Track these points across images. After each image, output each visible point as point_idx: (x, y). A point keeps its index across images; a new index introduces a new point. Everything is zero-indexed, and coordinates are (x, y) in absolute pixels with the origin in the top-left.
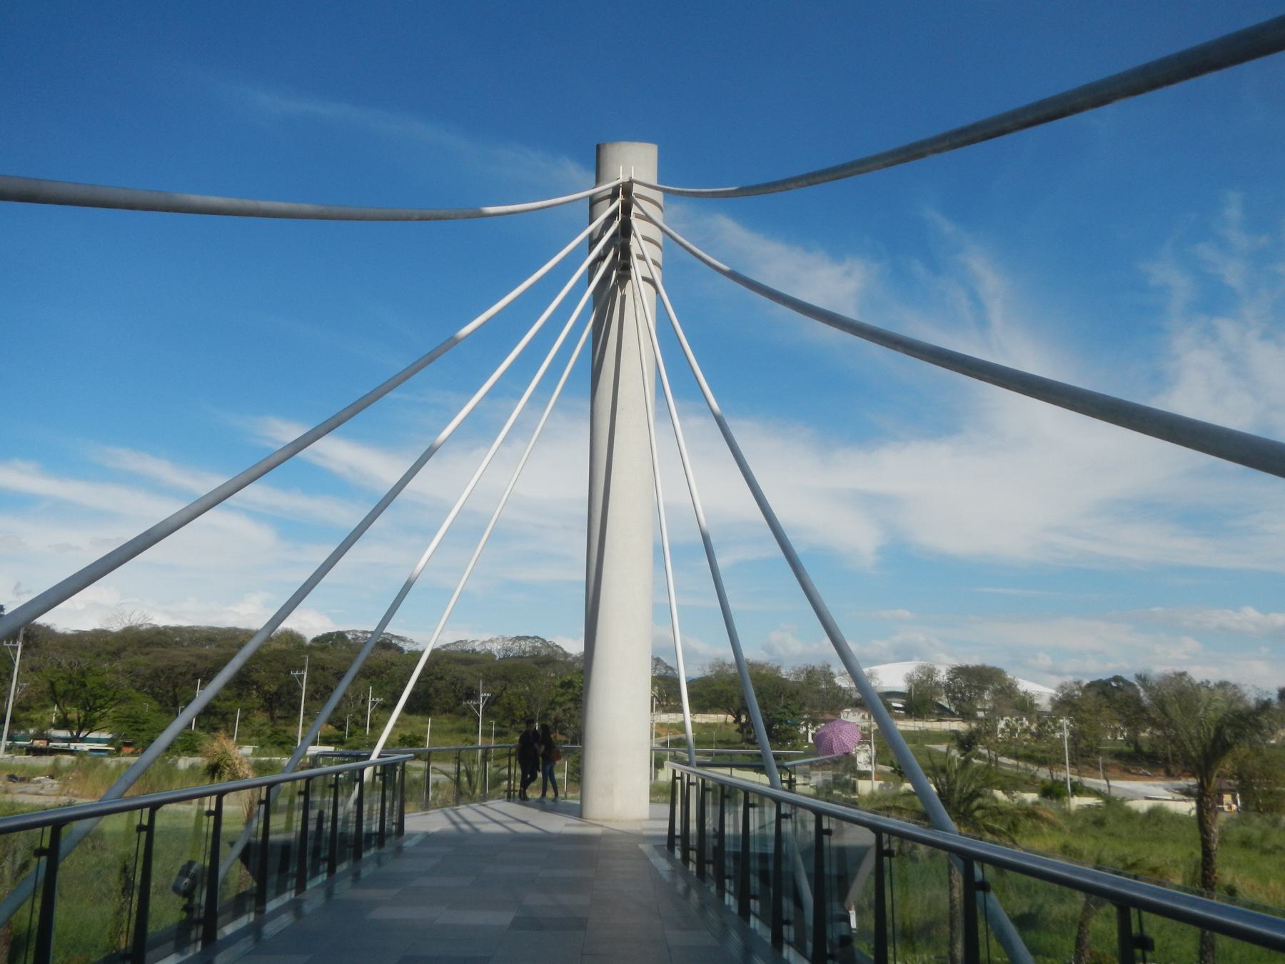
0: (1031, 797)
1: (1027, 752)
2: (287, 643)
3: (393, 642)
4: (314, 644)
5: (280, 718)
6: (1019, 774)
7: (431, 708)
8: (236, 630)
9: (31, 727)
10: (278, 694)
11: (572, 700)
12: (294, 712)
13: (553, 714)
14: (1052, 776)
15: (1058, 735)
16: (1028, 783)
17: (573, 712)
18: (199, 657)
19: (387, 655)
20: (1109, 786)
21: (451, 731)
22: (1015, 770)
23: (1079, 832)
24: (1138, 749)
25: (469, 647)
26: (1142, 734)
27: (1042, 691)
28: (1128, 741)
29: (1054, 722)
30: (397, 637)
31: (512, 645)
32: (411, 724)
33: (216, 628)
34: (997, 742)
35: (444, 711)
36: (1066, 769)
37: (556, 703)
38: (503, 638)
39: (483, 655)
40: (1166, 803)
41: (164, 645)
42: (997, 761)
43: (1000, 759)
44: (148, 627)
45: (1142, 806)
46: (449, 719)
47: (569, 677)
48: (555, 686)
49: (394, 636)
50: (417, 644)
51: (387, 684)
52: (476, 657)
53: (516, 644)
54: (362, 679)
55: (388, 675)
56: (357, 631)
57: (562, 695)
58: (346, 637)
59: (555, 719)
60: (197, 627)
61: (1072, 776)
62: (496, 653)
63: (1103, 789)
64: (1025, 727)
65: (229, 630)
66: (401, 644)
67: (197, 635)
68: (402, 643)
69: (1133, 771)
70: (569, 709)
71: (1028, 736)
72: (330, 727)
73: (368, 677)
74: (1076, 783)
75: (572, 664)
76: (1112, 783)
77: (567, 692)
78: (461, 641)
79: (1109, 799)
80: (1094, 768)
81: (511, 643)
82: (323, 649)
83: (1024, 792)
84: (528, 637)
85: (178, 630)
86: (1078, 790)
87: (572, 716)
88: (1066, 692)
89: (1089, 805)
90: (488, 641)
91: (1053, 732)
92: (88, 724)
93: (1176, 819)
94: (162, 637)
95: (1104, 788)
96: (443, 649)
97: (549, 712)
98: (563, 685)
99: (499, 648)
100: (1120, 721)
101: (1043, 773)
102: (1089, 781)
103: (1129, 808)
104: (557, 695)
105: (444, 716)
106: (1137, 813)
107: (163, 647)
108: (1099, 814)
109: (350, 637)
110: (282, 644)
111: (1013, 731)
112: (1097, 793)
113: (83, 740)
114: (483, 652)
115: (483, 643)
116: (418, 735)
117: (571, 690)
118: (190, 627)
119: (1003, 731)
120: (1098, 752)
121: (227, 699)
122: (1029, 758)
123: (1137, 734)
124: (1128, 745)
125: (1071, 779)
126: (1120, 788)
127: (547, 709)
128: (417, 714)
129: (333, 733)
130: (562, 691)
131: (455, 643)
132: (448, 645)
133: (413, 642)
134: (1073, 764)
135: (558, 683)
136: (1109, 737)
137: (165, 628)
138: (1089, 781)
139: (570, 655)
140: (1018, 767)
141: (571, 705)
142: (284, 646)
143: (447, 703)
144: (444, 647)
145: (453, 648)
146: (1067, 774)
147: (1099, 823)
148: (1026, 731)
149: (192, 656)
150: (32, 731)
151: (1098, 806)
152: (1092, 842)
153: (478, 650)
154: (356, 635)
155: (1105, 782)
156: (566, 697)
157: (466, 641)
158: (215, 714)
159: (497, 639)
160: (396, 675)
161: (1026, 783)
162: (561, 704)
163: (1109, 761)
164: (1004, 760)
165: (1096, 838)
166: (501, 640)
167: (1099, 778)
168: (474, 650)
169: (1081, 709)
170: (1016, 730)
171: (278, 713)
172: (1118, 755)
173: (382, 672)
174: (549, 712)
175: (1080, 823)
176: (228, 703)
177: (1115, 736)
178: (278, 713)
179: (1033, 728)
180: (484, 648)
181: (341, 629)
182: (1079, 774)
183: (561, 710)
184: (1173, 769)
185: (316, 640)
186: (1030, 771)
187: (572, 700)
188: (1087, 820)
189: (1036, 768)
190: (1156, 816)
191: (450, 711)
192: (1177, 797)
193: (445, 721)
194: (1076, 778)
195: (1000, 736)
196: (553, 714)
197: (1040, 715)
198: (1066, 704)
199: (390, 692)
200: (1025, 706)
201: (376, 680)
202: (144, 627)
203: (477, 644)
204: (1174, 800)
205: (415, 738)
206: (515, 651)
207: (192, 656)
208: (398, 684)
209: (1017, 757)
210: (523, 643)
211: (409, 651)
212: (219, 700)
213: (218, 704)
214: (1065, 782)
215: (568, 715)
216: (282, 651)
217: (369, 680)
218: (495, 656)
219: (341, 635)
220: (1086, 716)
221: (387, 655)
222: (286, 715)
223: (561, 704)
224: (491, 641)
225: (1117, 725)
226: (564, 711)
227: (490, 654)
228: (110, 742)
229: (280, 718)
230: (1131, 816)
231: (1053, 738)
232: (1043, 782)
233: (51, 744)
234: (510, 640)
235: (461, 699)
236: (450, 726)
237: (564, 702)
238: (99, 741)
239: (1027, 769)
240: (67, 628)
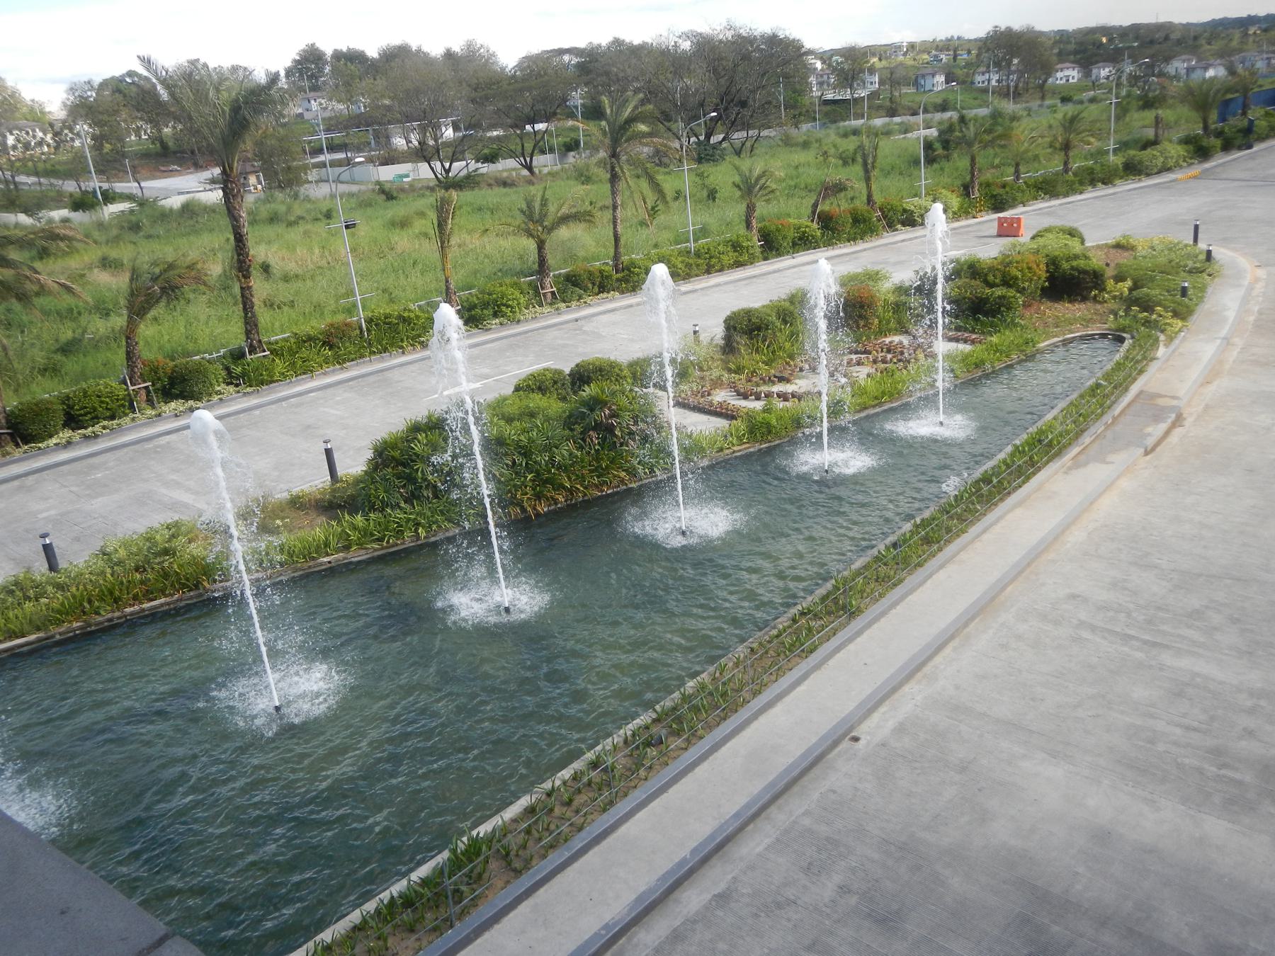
0: (58, 214)
1: (48, 166)
6: (42, 192)
14: (80, 188)
15: (77, 143)
16: (57, 200)
20: (141, 188)
22: (38, 188)
23: (116, 240)
24: (164, 146)
26: (166, 130)
27: (54, 103)
28: (153, 139)
29: (71, 130)
34: (9, 160)
36: (92, 178)
40: (198, 195)
42: (15, 183)
43: (18, 179)
45: (175, 202)
61: (101, 184)
63: (135, 192)
64: (38, 139)
69: (162, 168)
71: (46, 149)
74: (107, 190)
76: (143, 184)
79: (142, 203)
80: (120, 174)
83: (51, 210)
86: (109, 197)
88: (77, 94)
89: (122, 211)
91: (72, 140)
93: (210, 210)
95: (136, 191)
100: (142, 119)
101: (70, 186)
102: (120, 187)
103: (162, 206)
106: (171, 210)
108: (133, 218)
111: (27, 146)
112: (129, 197)
119: (14, 147)
120: (124, 155)
122: (52, 173)
123: (160, 131)
124: (153, 143)
125: (100, 188)
126: (153, 188)
134: (99, 172)
136: (133, 138)
138: (120, 187)
140: (40, 184)
146: (95, 183)
147: (135, 228)
148: (40, 143)
151: (132, 211)
152: (131, 247)
155: (136, 184)
161: (53, 199)
163: (136, 162)
164: (22, 179)
165: (134, 243)
167: (130, 182)
169: (100, 113)
170: (29, 143)
172: (146, 155)
175: (115, 232)
177: (138, 136)
179: (49, 138)
182: (108, 180)
184: (201, 162)
186: (55, 186)
188: (122, 228)
189: (61, 182)
190: (189, 210)
192: (208, 187)
194: (105, 186)
195: (12, 153)
197: (51, 125)
198: (82, 108)
200: (37, 117)
204: (205, 190)
209: (37, 174)
214: (94, 192)
220: (105, 117)
225: (139, 123)
230: (165, 216)
231: (72, 147)
232: (71, 195)
239: (51, 185)
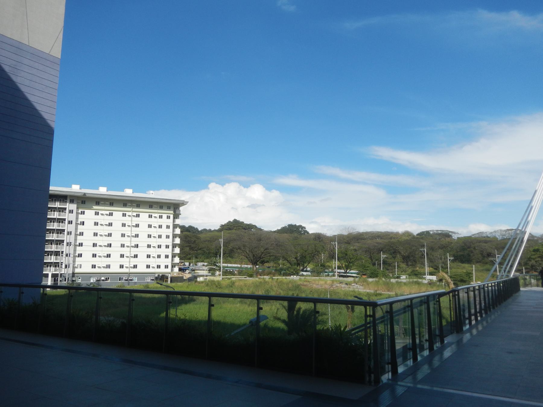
2: (408, 236)
3: (450, 234)
4: (418, 236)
5: (410, 265)
7: (471, 261)
8: (388, 232)
9: (330, 268)
10: (408, 257)
11: (539, 257)
12: (415, 263)
13: (530, 263)
17: (540, 262)
18: (377, 243)
19: (448, 239)
21: (483, 270)
25: (484, 235)
30: (452, 232)
31: (505, 233)
32: (464, 268)
33: (380, 232)
35: (477, 262)
37: (532, 258)
38: (501, 230)
39: (492, 238)
41: (364, 239)
44: (357, 233)
46: (480, 265)
47: (537, 248)
48: (530, 251)
49: (450, 232)
50: (460, 234)
51: (450, 251)
52: (488, 239)
53: (507, 232)
54: (440, 250)
55: (450, 247)
56: (434, 230)
57: (534, 255)
58: (430, 233)
59: (532, 265)
60: (373, 232)
62: (498, 237)
65: (385, 232)
66: (453, 235)
67: (374, 235)
68: (454, 234)
70: (538, 261)
72: (431, 268)
73: (442, 249)
75: (537, 240)
77: (536, 254)
78: (481, 233)
81: (504, 232)
82: (422, 238)
84: (513, 229)
85: (367, 233)
87: (540, 264)
90: (494, 232)
92: (347, 267)
94: (362, 236)
96: (473, 236)
97: (528, 262)
98: (535, 251)
99: (499, 234)
104: (532, 255)
105: (478, 264)
107: (364, 240)
109: (431, 233)
110: (406, 237)
113: (348, 273)
114: (491, 237)
115: (491, 233)
116: (469, 272)
117: (538, 253)
118: (370, 232)
121: (390, 259)
127: (527, 261)
128: (465, 263)
129: (433, 271)
130: (533, 253)
131: (478, 234)
132: (475, 234)
133: (458, 234)
135: (532, 249)
137: (363, 233)
139: (536, 237)
141: (539, 259)
142: (407, 238)
143: (478, 259)
144: (473, 235)
145: (477, 236)
149: (375, 243)
150: (330, 270)
153: (489, 236)
154: (434, 232)
156: (536, 256)
157: (483, 232)
158: (387, 264)
159: (498, 231)
160: (454, 248)
162: (534, 259)
166: (499, 231)
168: (487, 237)
171: (410, 263)
173: (447, 247)
174: (528, 262)
176: (390, 260)
178: (410, 263)
180: (492, 235)
181: (427, 230)
183: (534, 262)
185: (418, 235)
187: (539, 257)
191: (480, 262)
193: (479, 266)
196: (530, 263)
199: (452, 255)
201: (445, 250)
202: (356, 233)
203: (488, 233)
205: (468, 273)
206: (507, 236)
207: (375, 243)
208: (455, 251)
210: (510, 232)
211: (458, 238)
212: (388, 259)
213: (388, 260)
215: (538, 263)
216: (407, 240)
217: (443, 250)
218: (497, 238)
219: (428, 232)
221: (448, 239)
222: (412, 264)
223: (534, 259)
224: (495, 232)
226: (536, 261)
227: (495, 238)
228: (358, 274)
229: (410, 265)
233: (340, 274)
234: (504, 231)
235: (484, 257)
236: (482, 268)
237: (536, 258)
238: (352, 273)
240: (331, 235)
